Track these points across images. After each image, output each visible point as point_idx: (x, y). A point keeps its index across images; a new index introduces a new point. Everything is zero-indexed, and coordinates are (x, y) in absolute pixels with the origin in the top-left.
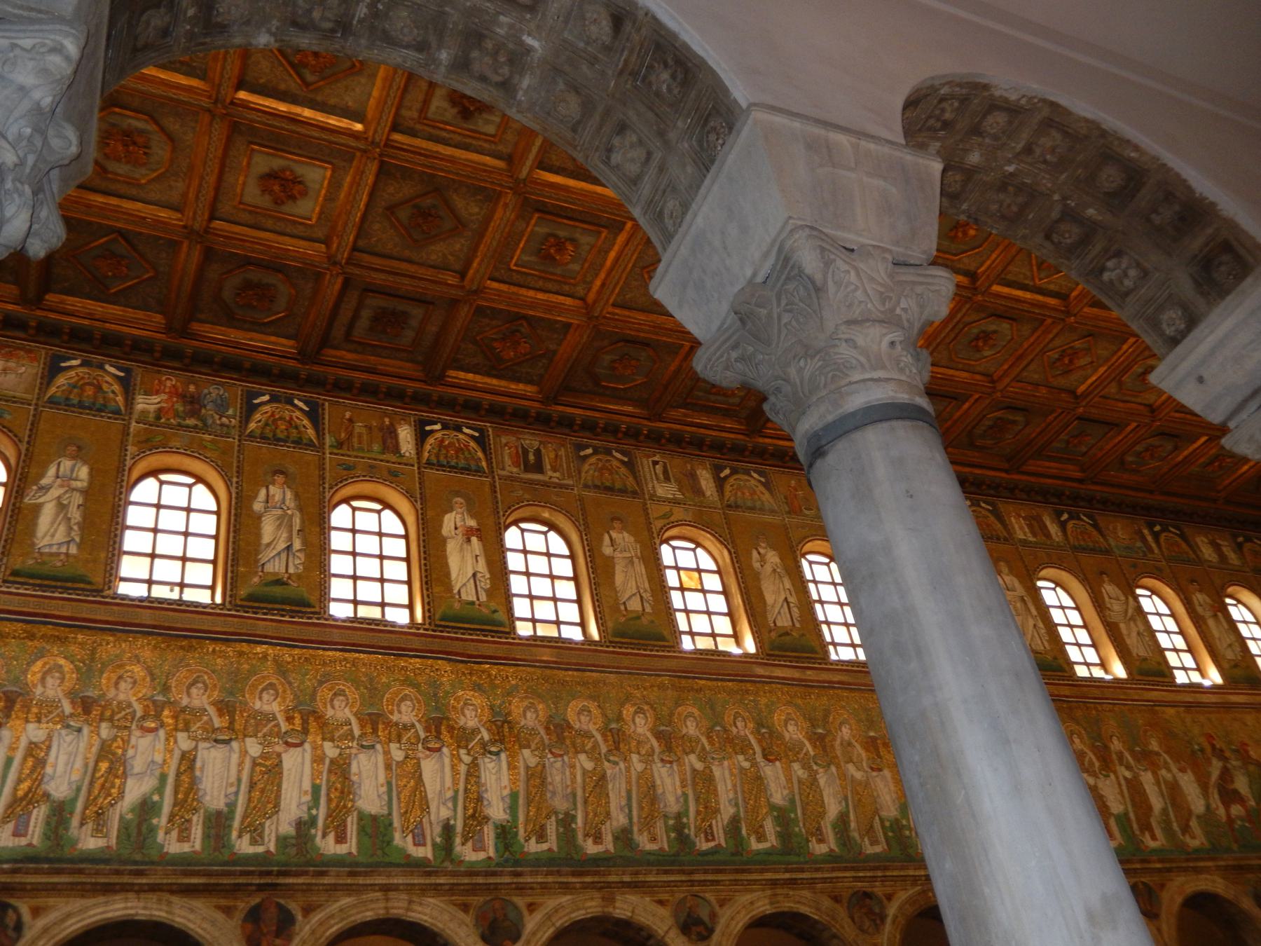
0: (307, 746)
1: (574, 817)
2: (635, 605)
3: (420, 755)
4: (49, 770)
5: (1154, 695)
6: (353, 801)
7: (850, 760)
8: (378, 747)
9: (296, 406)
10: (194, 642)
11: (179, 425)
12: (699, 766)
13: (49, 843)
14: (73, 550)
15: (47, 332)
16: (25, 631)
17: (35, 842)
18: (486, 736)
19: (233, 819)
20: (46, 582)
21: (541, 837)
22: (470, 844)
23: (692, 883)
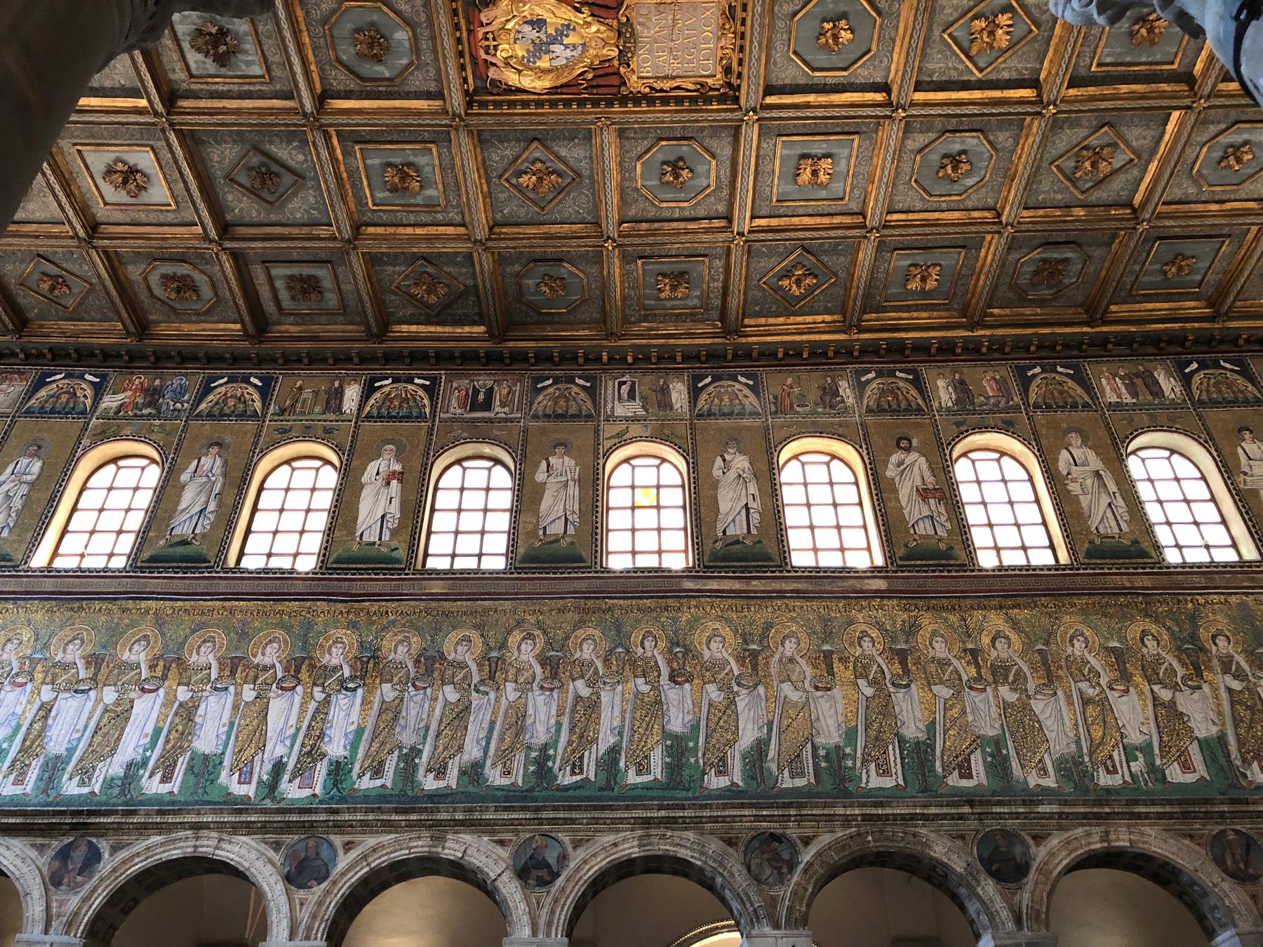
0: (161, 691)
1: (420, 751)
2: (557, 529)
6: (191, 741)
8: (232, 689)
11: (135, 415)
15: (32, 357)
18: (347, 672)
19: (68, 764)
21: (377, 772)
22: (297, 781)
23: (541, 821)
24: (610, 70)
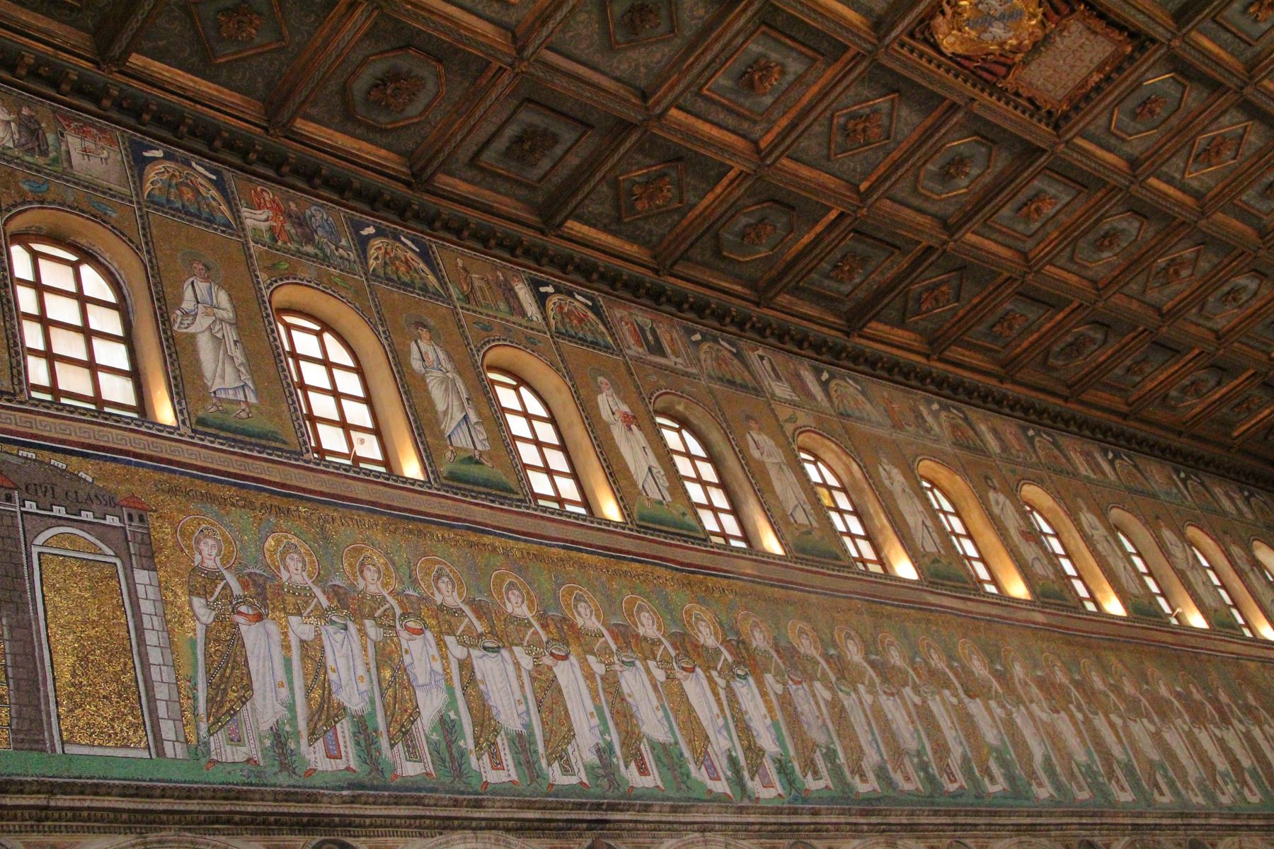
0: (573, 658)
1: (835, 751)
3: (679, 675)
4: (333, 676)
5: (1232, 647)
7: (1032, 701)
8: (638, 663)
9: (405, 244)
10: (421, 526)
12: (917, 700)
13: (367, 768)
14: (252, 399)
16: (243, 499)
17: (352, 766)
18: (730, 659)
19: (535, 743)
20: (239, 437)
24: (1009, 62)
